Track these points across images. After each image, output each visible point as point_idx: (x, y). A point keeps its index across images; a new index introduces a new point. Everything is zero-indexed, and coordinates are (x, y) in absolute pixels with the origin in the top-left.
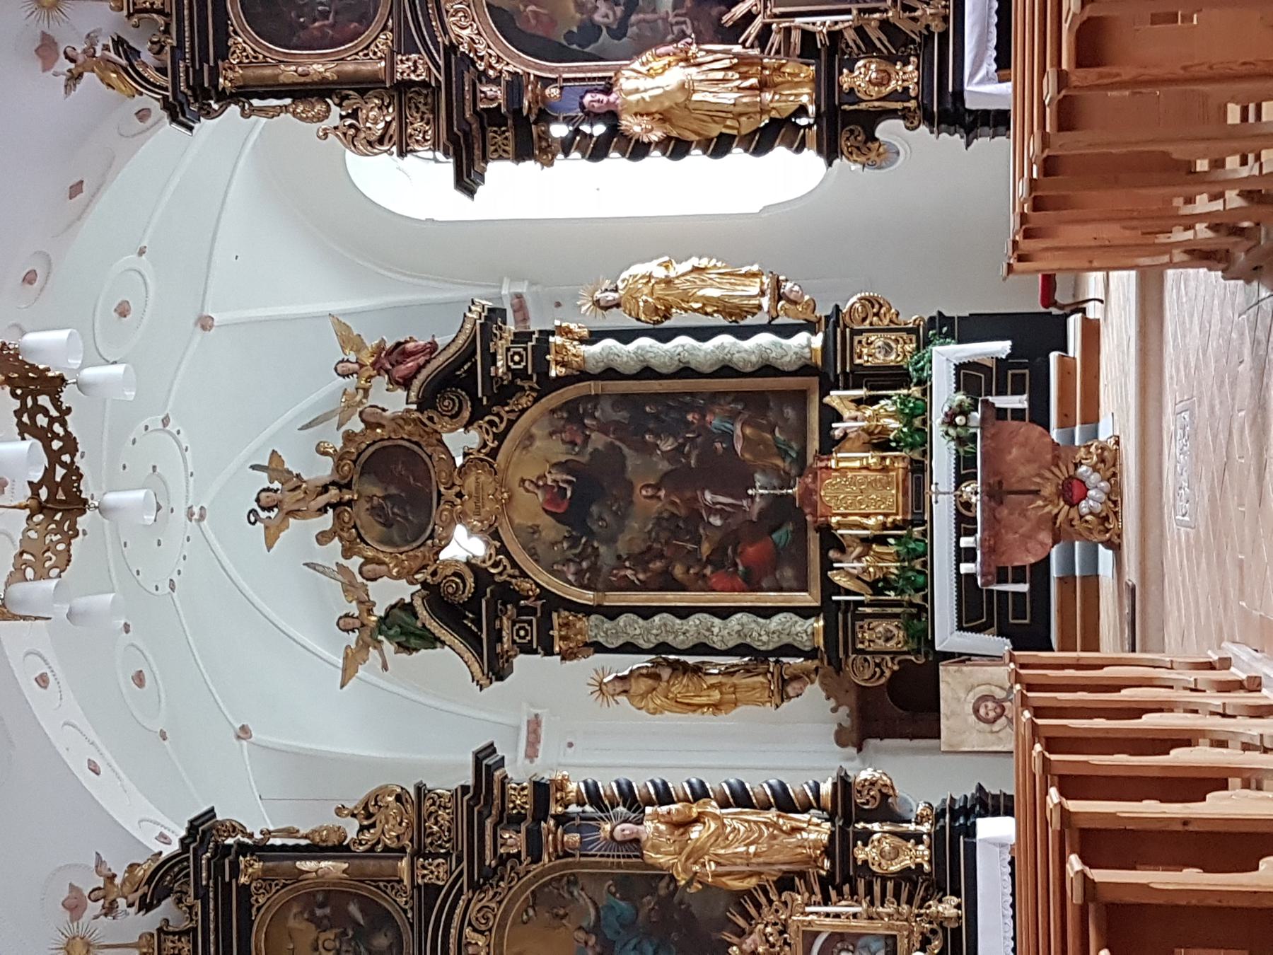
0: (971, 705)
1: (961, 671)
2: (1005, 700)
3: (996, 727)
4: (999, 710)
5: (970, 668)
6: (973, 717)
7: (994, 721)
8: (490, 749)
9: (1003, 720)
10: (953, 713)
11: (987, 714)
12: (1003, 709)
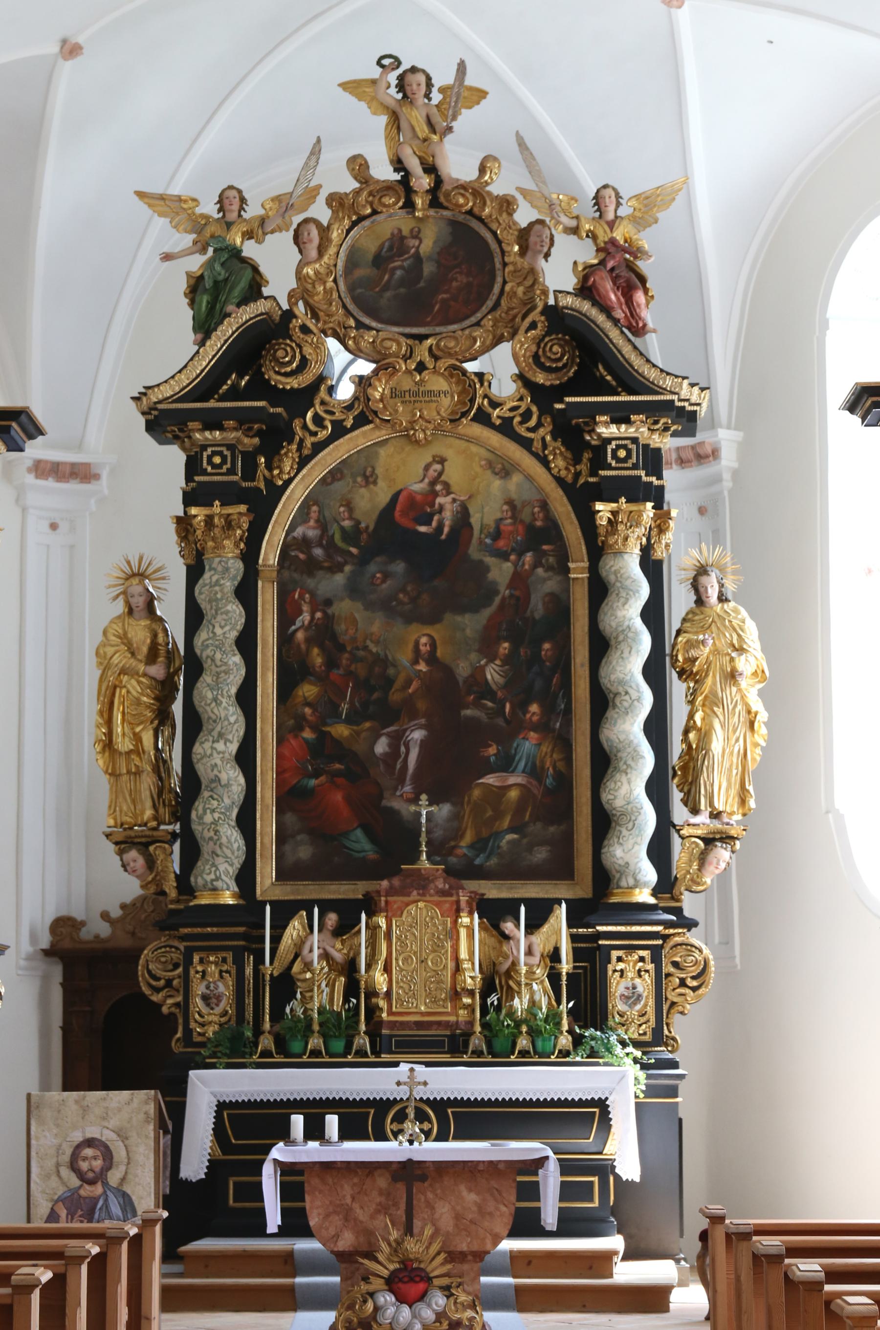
0: (97, 1136)
1: (147, 1121)
2: (105, 1184)
3: (65, 1172)
4: (91, 1175)
5: (152, 1135)
6: (81, 1139)
7: (73, 1166)
8: (34, 430)
9: (75, 1182)
10: (85, 1110)
11: (85, 1159)
12: (92, 1182)
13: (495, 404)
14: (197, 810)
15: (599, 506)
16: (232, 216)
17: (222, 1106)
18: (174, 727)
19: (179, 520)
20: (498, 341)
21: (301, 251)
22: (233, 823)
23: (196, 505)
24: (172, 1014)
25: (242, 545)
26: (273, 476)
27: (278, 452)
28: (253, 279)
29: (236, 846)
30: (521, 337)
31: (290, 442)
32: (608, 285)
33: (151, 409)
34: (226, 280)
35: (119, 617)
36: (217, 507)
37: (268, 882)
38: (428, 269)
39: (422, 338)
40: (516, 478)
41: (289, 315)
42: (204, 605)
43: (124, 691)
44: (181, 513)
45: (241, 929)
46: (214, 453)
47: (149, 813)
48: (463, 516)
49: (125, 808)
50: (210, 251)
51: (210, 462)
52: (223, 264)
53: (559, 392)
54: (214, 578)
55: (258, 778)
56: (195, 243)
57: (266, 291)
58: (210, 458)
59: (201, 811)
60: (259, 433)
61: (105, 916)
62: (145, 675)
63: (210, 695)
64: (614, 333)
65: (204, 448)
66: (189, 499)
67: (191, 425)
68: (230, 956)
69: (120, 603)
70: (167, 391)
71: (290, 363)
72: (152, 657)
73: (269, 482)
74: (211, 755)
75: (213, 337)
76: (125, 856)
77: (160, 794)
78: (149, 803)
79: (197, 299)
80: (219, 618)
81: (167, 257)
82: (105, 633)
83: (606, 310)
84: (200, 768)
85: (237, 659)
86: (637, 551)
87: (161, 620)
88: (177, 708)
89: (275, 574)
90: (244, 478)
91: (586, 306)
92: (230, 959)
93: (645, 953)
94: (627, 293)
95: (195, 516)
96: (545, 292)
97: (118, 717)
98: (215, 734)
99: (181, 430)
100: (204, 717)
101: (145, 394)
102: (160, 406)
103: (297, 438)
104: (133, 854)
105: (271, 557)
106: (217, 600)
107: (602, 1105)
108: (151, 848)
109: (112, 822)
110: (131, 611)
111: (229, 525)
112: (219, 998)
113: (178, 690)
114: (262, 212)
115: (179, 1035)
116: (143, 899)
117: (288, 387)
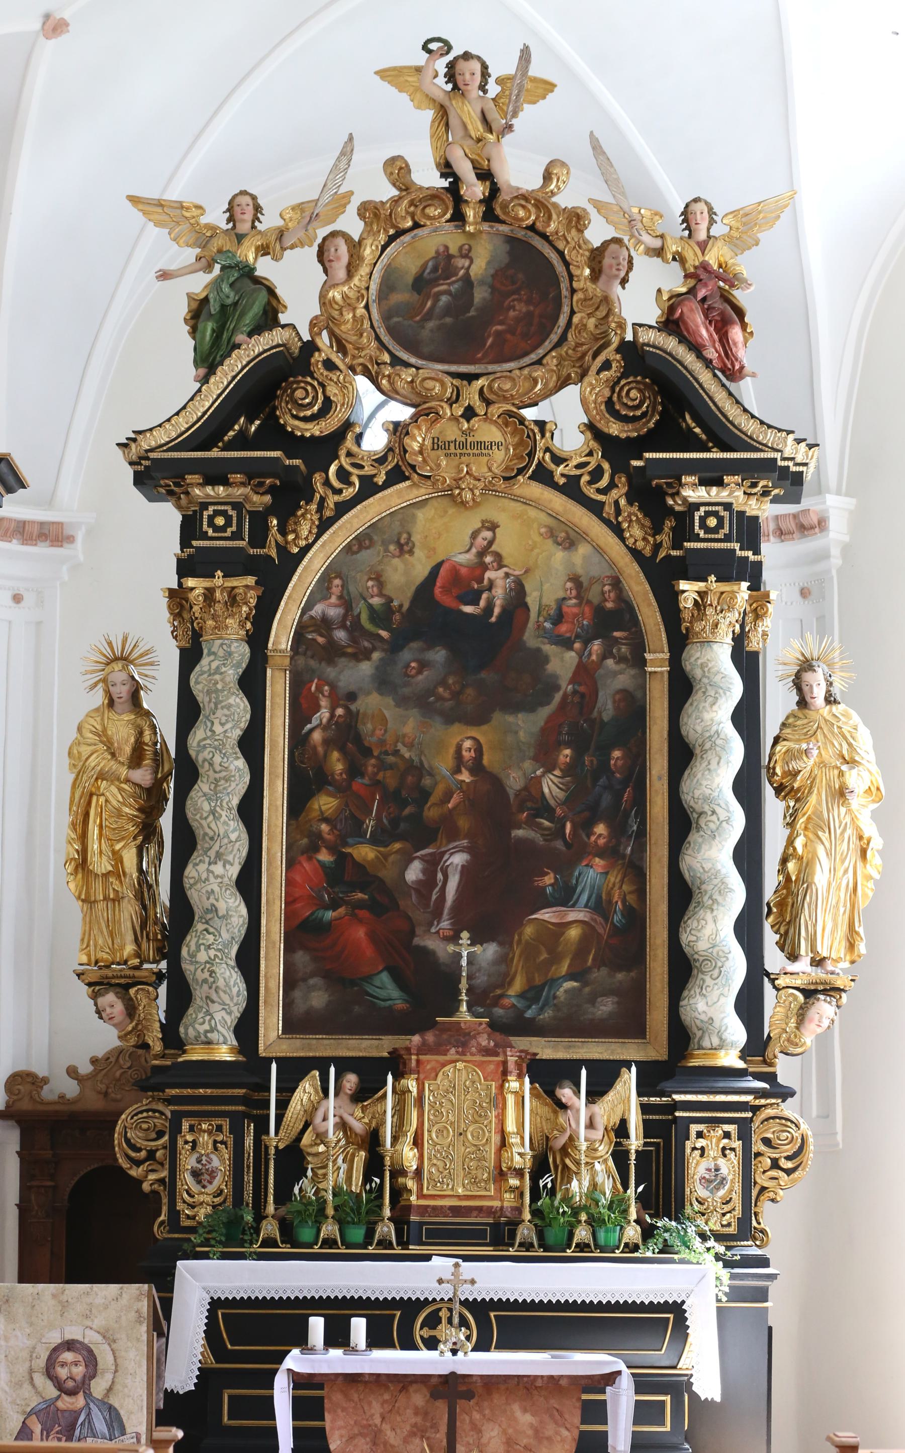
13: (558, 460)
15: (683, 585)
16: (243, 228)
17: (216, 1304)
18: (161, 844)
19: (172, 593)
20: (563, 383)
21: (326, 271)
22: (233, 963)
23: (194, 575)
24: (155, 1193)
25: (249, 626)
26: (287, 542)
27: (294, 514)
28: (269, 303)
29: (235, 990)
30: (591, 378)
31: (309, 501)
32: (699, 318)
33: (141, 458)
34: (236, 304)
35: (97, 710)
36: (219, 579)
37: (273, 1035)
38: (480, 295)
39: (471, 378)
40: (583, 550)
41: (310, 347)
42: (200, 697)
43: (102, 799)
45: (241, 1092)
46: (217, 513)
47: (130, 948)
48: (518, 594)
49: (100, 942)
50: (217, 267)
51: (211, 523)
52: (232, 285)
53: (637, 446)
54: (214, 665)
55: (264, 909)
56: (199, 259)
57: (283, 318)
58: (211, 519)
59: (193, 947)
60: (272, 490)
61: (72, 1072)
62: (127, 781)
63: (206, 807)
64: (705, 377)
65: (204, 506)
66: (185, 568)
67: (190, 478)
68: (226, 1124)
69: (100, 691)
70: (161, 437)
71: (311, 405)
72: (136, 759)
73: (282, 550)
74: (207, 879)
75: (219, 373)
76: (100, 1000)
77: (143, 925)
78: (130, 937)
79: (200, 326)
80: (219, 713)
81: (164, 275)
82: (80, 729)
83: (697, 349)
84: (194, 896)
85: (240, 763)
86: (729, 640)
87: (148, 714)
88: (166, 822)
89: (287, 661)
90: (252, 544)
91: (671, 343)
92: (226, 1128)
93: (732, 1128)
94: (722, 328)
95: (192, 589)
96: (621, 326)
97: (94, 831)
98: (212, 854)
99: (177, 485)
100: (199, 833)
101: (134, 440)
102: (152, 455)
103: (317, 496)
104: (110, 997)
105: (283, 640)
106: (217, 691)
107: (677, 1309)
108: (132, 991)
109: (84, 959)
110: (111, 703)
111: (233, 600)
112: (212, 1174)
113: (167, 800)
114: (280, 223)
115: (162, 1218)
116: (119, 1052)
117: (308, 435)
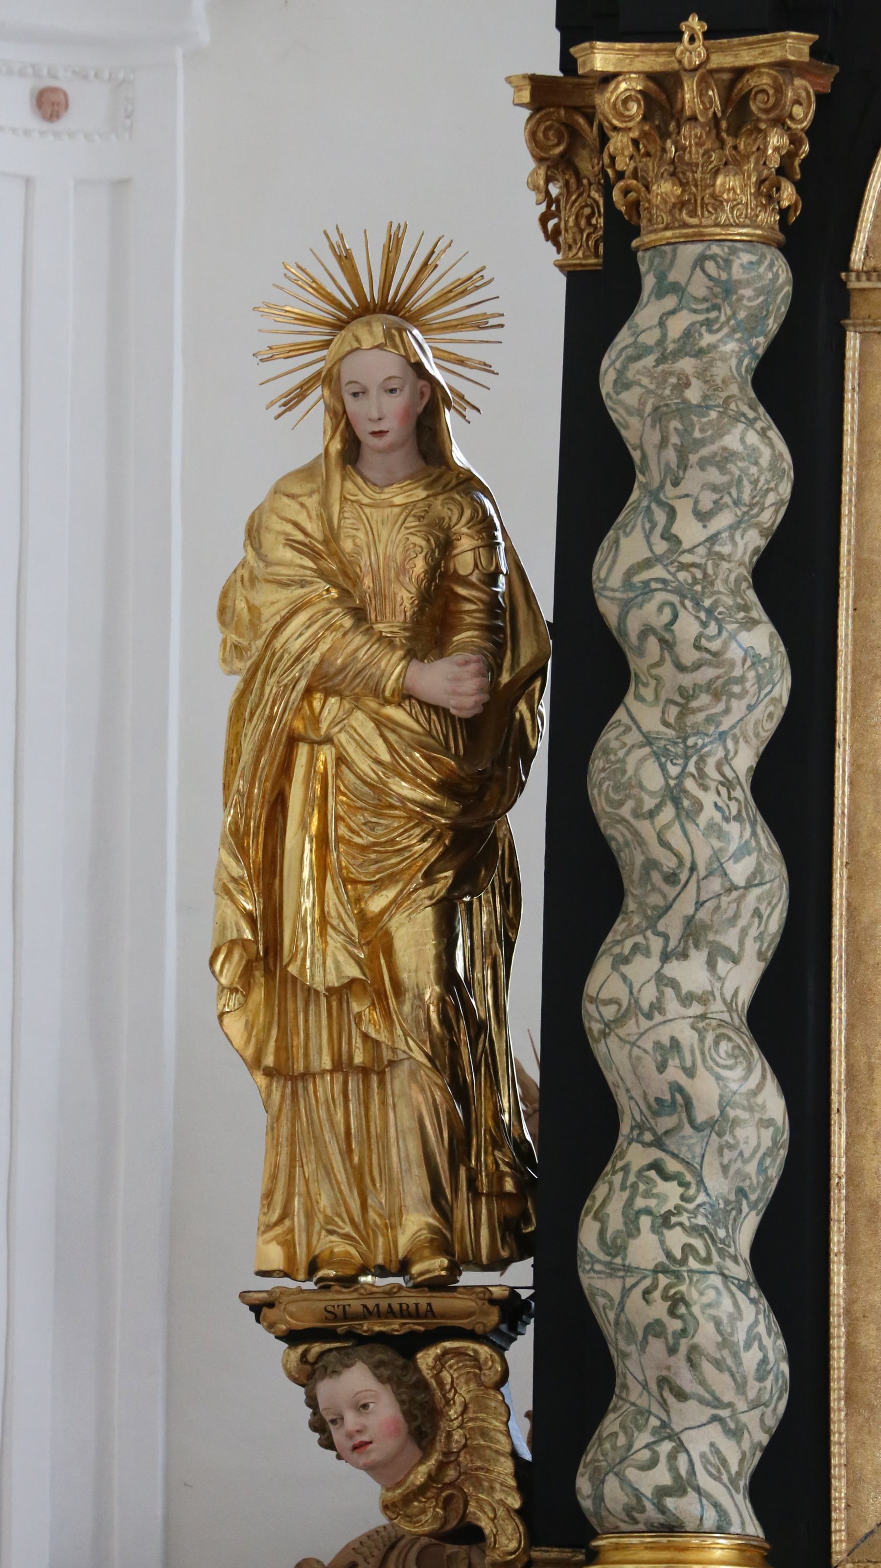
14: (600, 1217)
22: (742, 1271)
25: (788, 194)
29: (751, 1359)
35: (308, 472)
43: (326, 754)
44: (552, 68)
49: (324, 1202)
54: (677, 326)
55: (838, 1098)
59: (616, 1222)
74: (657, 1006)
76: (325, 1389)
95: (607, 78)
98: (672, 924)
106: (685, 410)
108: (426, 1359)
109: (275, 1257)
113: (529, 755)
